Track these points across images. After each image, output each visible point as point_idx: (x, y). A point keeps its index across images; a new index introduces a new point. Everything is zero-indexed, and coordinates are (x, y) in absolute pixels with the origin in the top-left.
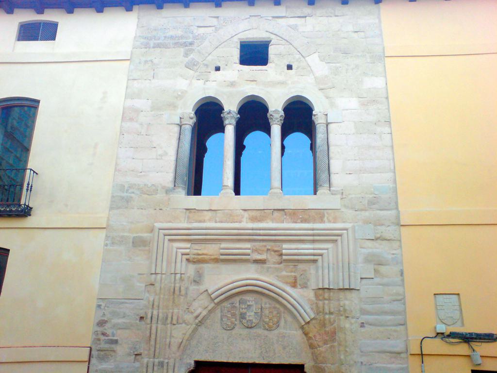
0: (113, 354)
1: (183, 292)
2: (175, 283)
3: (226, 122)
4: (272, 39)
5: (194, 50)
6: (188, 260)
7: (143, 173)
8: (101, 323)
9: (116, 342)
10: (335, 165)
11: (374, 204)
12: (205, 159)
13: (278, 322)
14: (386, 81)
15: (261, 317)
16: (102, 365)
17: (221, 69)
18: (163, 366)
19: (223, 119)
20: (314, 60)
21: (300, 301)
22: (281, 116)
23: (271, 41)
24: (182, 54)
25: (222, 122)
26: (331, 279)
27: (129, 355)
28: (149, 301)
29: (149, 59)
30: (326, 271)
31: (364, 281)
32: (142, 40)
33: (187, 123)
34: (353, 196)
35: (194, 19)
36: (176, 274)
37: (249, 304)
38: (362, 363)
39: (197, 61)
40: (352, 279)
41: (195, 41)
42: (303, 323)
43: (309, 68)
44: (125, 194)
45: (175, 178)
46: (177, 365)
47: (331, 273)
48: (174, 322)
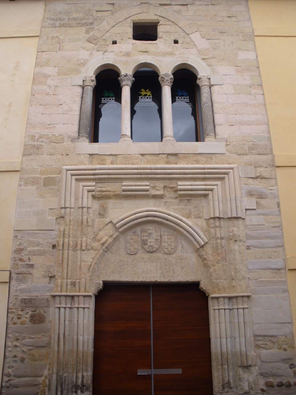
0: (30, 276)
1: (90, 223)
2: (82, 216)
3: (124, 83)
4: (160, 20)
5: (94, 28)
6: (94, 197)
7: (51, 126)
8: (19, 251)
9: (32, 266)
10: (219, 118)
11: (253, 150)
12: (100, 123)
13: (176, 247)
14: (257, 54)
15: (161, 244)
16: (21, 286)
17: (117, 43)
18: (75, 286)
19: (120, 82)
20: (196, 37)
21: (195, 228)
22: (171, 79)
23: (159, 22)
24: (84, 31)
25: (120, 84)
26: (221, 210)
27: (45, 277)
28: (60, 231)
29: (56, 35)
30: (217, 203)
31: (248, 212)
32: (49, 21)
33: (89, 84)
34: (236, 143)
35: (94, 5)
36: (83, 208)
37: (149, 232)
38: (249, 278)
39: (96, 36)
40: (239, 209)
41: (95, 22)
42: (198, 247)
43: (193, 43)
44: (36, 143)
45: (79, 129)
46: (88, 284)
47: (221, 205)
48: (84, 248)
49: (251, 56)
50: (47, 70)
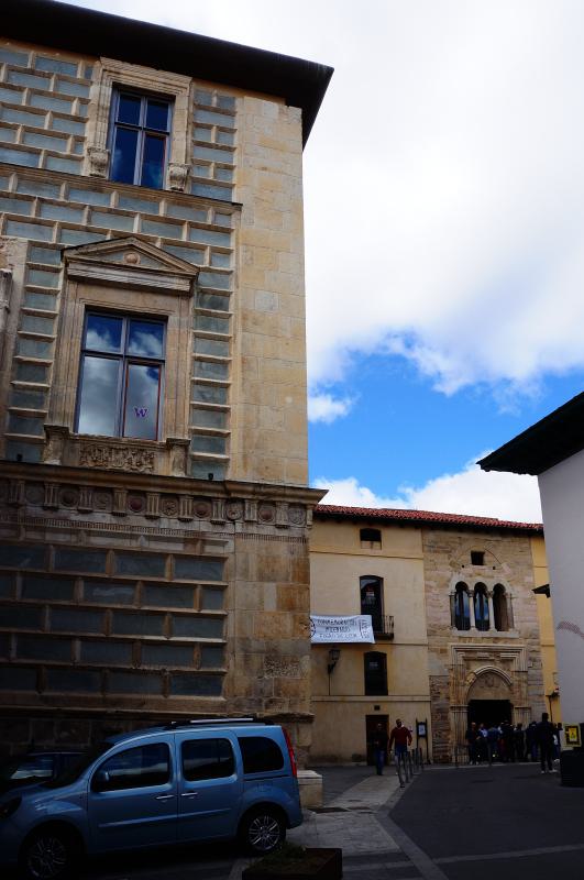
20: (504, 566)
49: (531, 579)
50: (432, 584)
